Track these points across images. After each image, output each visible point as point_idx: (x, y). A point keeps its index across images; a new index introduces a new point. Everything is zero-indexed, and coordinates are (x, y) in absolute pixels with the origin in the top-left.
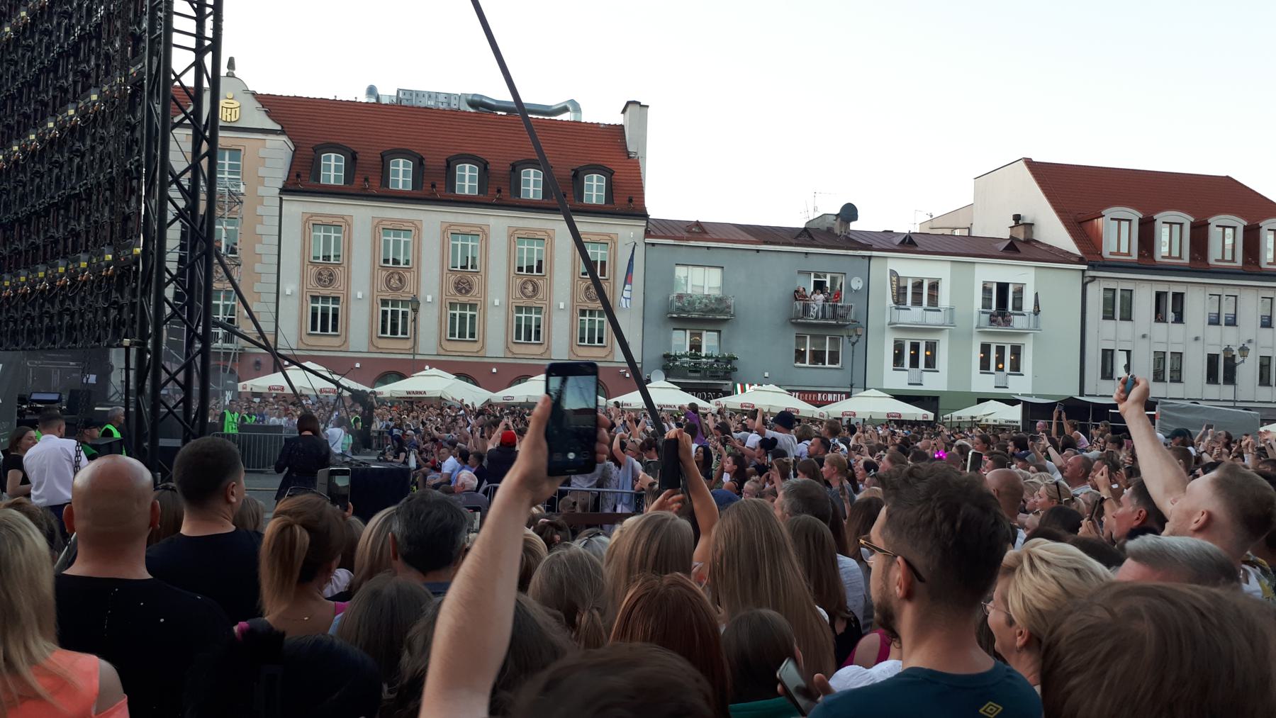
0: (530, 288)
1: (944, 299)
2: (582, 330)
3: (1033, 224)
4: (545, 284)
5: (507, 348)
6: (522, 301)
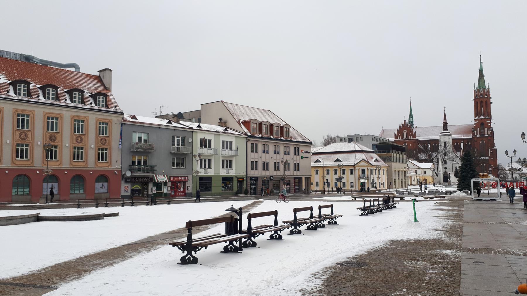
0: (79, 139)
1: (213, 146)
2: (74, 154)
3: (226, 122)
4: (31, 134)
5: (71, 163)
6: (76, 144)
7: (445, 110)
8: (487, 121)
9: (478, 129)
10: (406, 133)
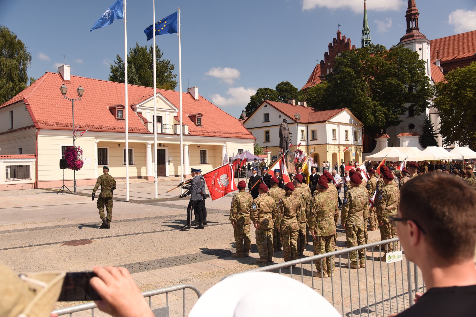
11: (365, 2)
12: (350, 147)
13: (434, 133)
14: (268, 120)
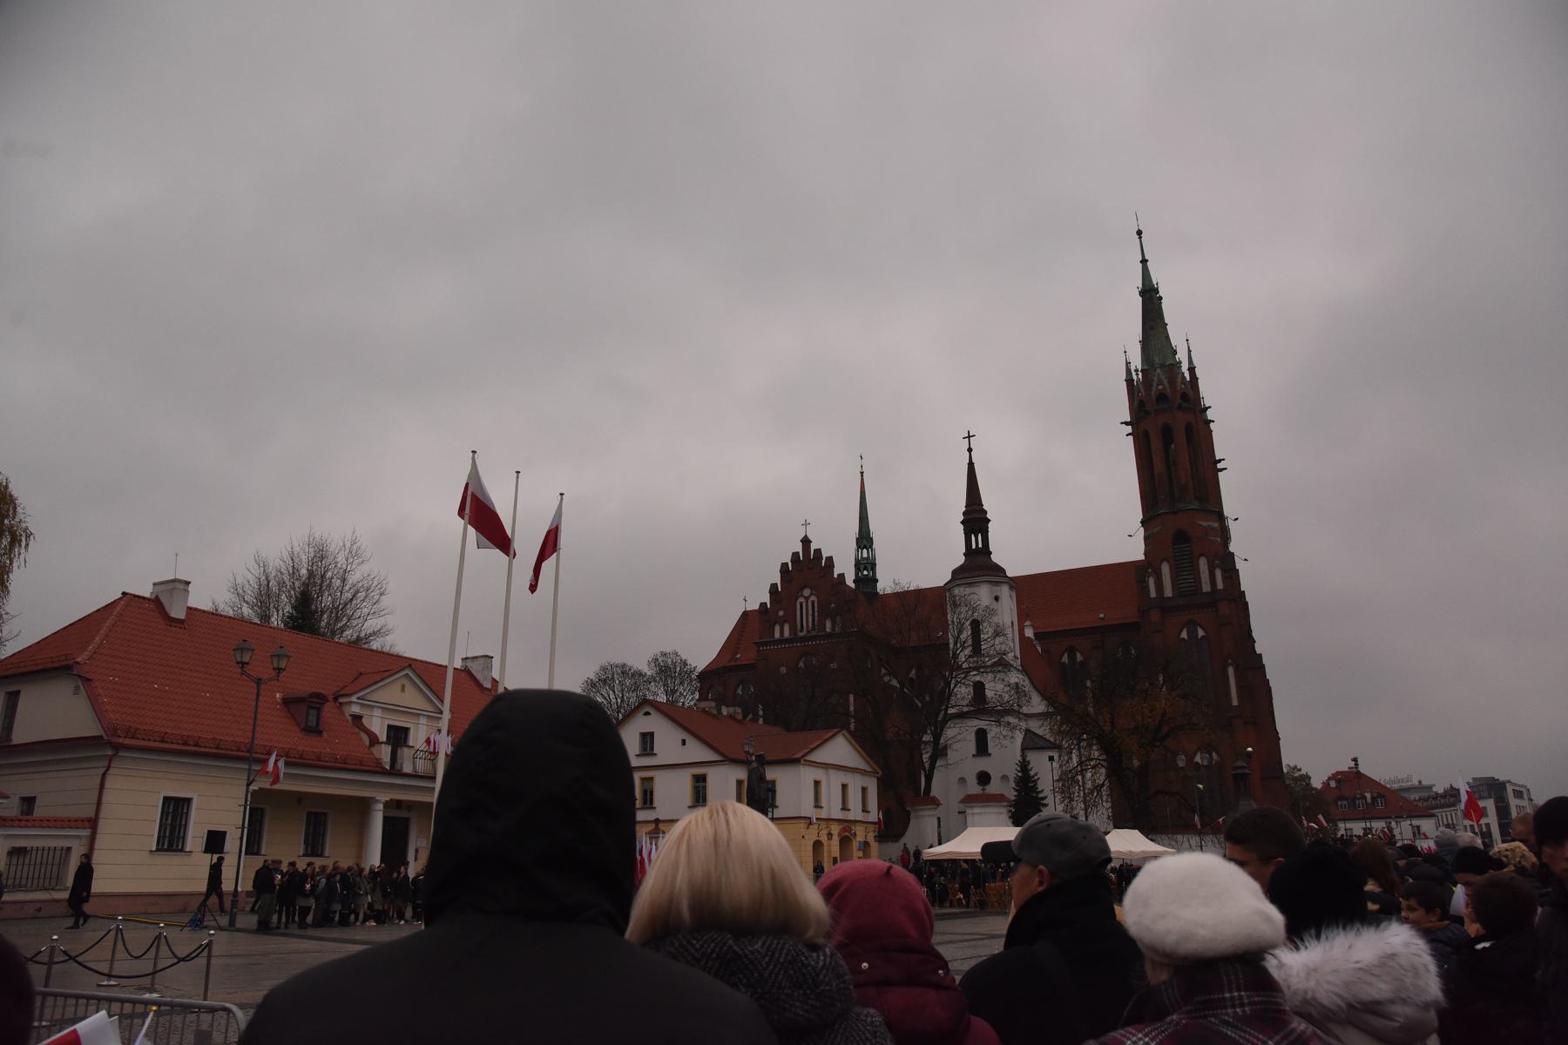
7: (970, 450)
8: (1204, 524)
9: (1165, 569)
10: (813, 603)
11: (862, 476)
12: (853, 828)
13: (1040, 796)
14: (652, 748)
